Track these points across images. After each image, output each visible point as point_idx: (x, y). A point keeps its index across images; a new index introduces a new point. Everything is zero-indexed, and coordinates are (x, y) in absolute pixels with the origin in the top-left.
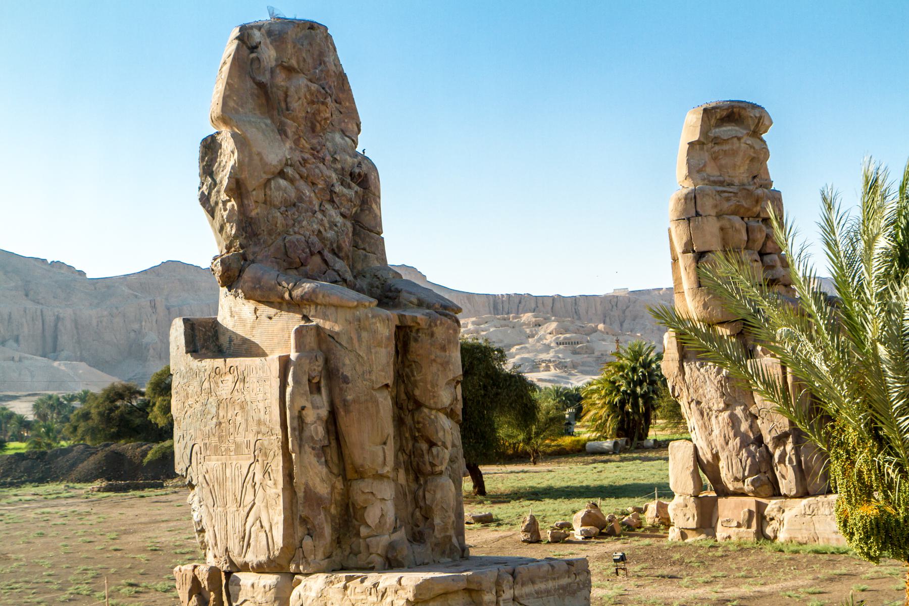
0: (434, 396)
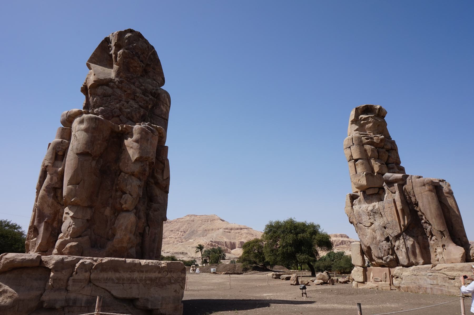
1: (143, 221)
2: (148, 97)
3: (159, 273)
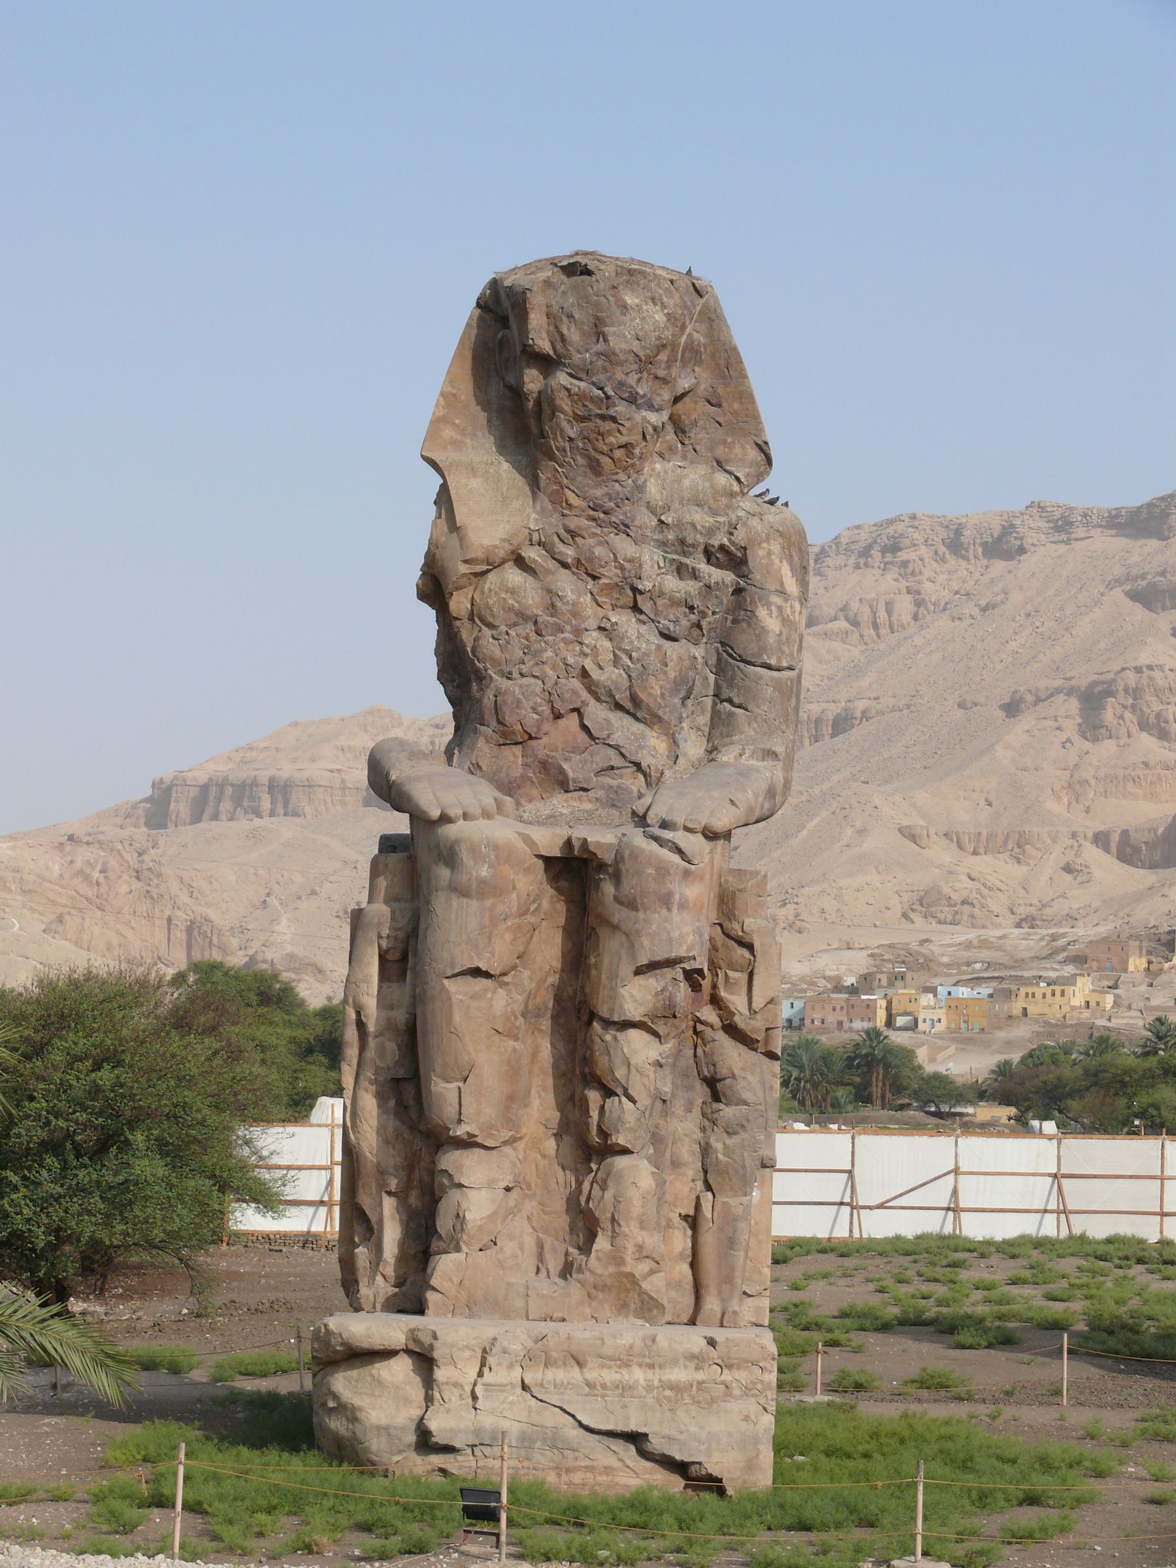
0: (611, 997)
1: (690, 1173)
2: (694, 575)
3: (697, 1369)
